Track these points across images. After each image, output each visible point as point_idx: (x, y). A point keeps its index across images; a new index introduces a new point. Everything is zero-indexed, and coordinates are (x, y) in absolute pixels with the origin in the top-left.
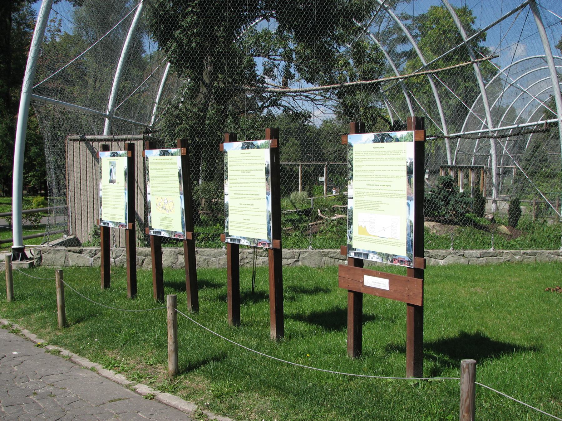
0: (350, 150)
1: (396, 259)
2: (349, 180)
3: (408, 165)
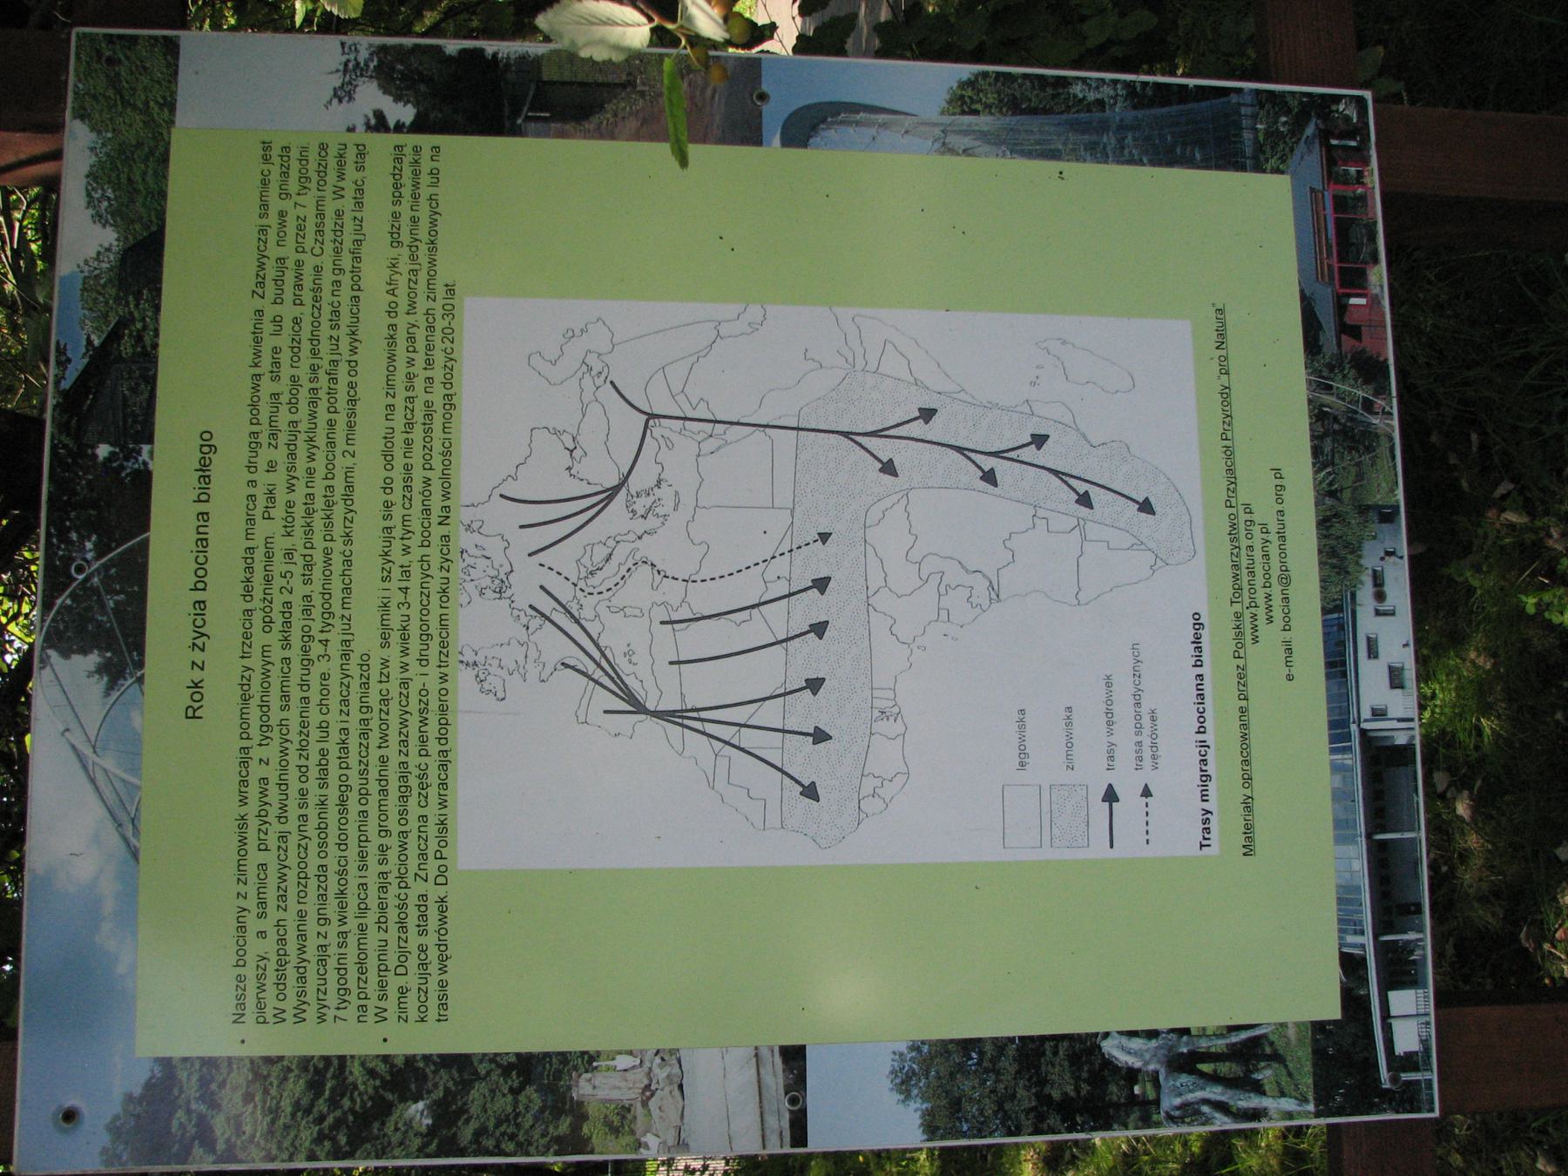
0: (205, 1136)
1: (1341, 308)
2: (577, 1142)
3: (405, 113)
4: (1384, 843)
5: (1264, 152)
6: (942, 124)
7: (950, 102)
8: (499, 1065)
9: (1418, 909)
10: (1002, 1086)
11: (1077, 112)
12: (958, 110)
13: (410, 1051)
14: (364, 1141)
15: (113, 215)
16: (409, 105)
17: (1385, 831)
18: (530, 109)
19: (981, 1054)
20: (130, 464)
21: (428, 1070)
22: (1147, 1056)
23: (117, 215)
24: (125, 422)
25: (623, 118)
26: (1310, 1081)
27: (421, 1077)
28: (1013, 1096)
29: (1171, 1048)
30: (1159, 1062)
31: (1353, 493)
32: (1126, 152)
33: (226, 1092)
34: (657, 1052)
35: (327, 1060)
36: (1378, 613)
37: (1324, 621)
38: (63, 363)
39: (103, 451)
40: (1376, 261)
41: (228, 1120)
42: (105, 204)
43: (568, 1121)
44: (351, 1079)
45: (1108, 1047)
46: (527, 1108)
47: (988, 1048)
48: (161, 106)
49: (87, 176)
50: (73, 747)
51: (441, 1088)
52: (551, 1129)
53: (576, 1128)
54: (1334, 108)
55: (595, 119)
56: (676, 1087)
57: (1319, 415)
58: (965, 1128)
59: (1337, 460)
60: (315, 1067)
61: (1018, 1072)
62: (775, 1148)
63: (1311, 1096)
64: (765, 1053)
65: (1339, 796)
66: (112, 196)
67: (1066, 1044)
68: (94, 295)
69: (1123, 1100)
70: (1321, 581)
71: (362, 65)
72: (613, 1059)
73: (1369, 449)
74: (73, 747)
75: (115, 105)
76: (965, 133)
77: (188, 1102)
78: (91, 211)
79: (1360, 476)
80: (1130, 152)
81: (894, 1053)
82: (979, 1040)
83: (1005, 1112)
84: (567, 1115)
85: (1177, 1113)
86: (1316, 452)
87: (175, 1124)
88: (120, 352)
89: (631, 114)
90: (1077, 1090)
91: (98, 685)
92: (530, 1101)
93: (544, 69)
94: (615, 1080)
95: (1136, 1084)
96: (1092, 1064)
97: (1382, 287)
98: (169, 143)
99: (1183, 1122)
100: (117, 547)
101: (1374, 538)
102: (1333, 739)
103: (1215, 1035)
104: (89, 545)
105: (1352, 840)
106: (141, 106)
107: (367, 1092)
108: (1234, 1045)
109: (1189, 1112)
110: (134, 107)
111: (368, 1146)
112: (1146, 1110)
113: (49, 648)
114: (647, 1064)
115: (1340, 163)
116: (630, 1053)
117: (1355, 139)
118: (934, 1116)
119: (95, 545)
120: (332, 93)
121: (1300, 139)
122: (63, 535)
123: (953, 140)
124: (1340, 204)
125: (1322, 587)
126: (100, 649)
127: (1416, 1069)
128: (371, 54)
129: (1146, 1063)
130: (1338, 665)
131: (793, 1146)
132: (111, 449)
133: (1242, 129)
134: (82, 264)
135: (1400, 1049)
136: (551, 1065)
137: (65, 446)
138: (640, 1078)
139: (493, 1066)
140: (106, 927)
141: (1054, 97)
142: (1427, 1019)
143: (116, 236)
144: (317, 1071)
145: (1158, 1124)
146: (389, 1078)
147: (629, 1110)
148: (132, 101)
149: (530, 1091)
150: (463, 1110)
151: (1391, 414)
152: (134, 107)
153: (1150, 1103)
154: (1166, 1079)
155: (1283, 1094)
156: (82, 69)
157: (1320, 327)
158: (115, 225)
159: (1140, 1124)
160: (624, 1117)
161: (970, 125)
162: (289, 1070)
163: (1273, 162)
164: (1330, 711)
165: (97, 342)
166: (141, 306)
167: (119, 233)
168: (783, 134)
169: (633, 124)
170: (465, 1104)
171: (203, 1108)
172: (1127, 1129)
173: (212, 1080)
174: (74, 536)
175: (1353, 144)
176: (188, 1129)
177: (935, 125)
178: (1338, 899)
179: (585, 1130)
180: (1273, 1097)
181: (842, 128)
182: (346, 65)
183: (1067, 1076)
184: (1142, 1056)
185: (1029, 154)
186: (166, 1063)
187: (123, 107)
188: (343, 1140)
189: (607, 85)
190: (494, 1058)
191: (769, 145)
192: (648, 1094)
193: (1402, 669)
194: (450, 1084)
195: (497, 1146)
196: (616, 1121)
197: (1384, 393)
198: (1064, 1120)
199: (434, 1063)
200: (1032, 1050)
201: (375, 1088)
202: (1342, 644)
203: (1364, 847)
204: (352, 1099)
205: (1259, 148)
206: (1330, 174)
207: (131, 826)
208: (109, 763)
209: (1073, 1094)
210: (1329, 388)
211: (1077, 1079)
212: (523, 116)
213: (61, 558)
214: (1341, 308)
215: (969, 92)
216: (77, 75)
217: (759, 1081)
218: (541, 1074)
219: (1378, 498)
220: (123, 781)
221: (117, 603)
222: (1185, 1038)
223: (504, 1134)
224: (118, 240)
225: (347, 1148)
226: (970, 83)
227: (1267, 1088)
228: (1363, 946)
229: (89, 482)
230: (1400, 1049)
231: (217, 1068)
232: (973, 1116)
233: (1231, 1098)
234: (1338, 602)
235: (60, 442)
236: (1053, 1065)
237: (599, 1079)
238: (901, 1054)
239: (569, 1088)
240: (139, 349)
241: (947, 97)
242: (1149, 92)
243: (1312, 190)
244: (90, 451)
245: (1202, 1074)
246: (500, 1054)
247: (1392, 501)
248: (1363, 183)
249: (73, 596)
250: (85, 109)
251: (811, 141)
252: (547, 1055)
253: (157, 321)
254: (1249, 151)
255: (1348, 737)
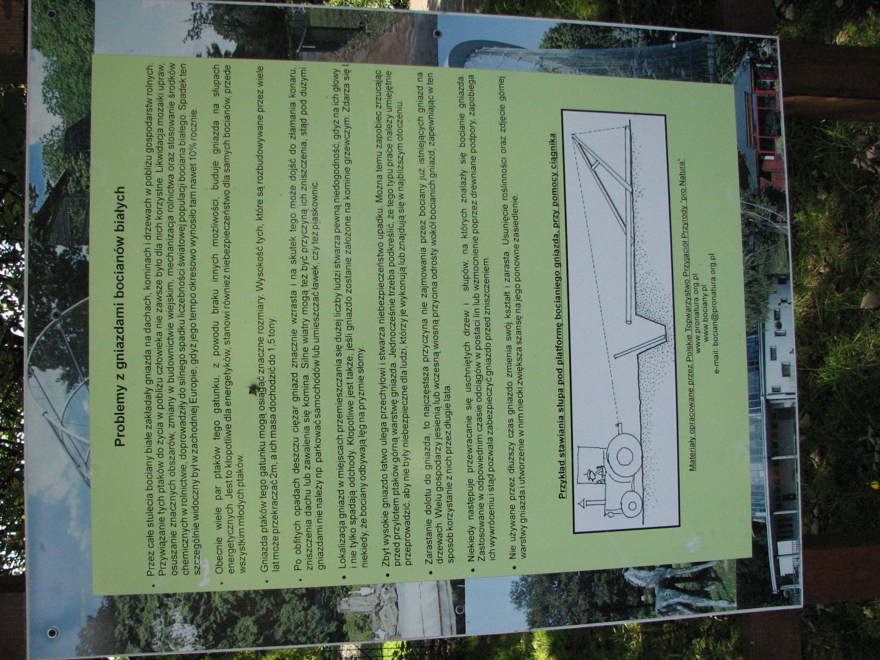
1: (760, 162)
3: (231, 46)
4: (777, 461)
5: (719, 71)
6: (540, 54)
7: (545, 41)
8: (296, 595)
9: (794, 497)
10: (570, 599)
11: (616, 47)
12: (549, 45)
13: (247, 588)
14: (224, 638)
15: (59, 108)
16: (233, 41)
17: (778, 455)
18: (304, 44)
19: (560, 582)
20: (75, 257)
21: (257, 599)
22: (649, 580)
23: (63, 108)
24: (72, 232)
25: (358, 50)
26: (735, 591)
27: (253, 603)
28: (576, 604)
29: (661, 575)
30: (655, 583)
31: (764, 267)
32: (643, 71)
33: (145, 614)
34: (384, 585)
35: (201, 595)
36: (777, 335)
37: (747, 339)
38: (34, 197)
39: (60, 249)
40: (780, 134)
41: (146, 629)
42: (54, 101)
43: (335, 624)
44: (214, 605)
45: (628, 576)
46: (312, 618)
47: (563, 578)
48: (86, 41)
49: (43, 84)
50: (50, 423)
51: (265, 608)
52: (326, 629)
53: (339, 628)
54: (759, 45)
55: (342, 50)
56: (394, 603)
57: (747, 223)
58: (551, 621)
59: (756, 249)
60: (194, 598)
61: (579, 591)
62: (447, 635)
63: (735, 600)
64: (442, 583)
65: (753, 436)
66: (58, 96)
67: (605, 575)
68: (51, 156)
69: (635, 604)
70: (746, 317)
71: (204, 16)
72: (359, 590)
73: (774, 242)
74: (50, 423)
75: (58, 40)
76: (554, 59)
77: (124, 620)
78: (46, 106)
79: (768, 258)
80: (646, 72)
81: (513, 582)
82: (559, 574)
83: (572, 612)
84: (334, 621)
85: (664, 610)
86: (745, 244)
87: (117, 632)
88: (67, 190)
89: (362, 47)
90: (611, 599)
91: (62, 387)
92: (314, 614)
93: (311, 19)
94: (361, 601)
95: (642, 594)
96: (619, 585)
97: (783, 149)
98: (91, 64)
99: (668, 615)
100: (69, 307)
101: (776, 292)
102: (751, 405)
103: (685, 567)
104: (54, 305)
105: (760, 460)
106: (73, 40)
107: (223, 611)
108: (696, 572)
109: (670, 609)
110: (69, 42)
111: (225, 641)
112: (648, 609)
113: (33, 365)
114: (378, 592)
115: (761, 77)
116: (369, 586)
117: (769, 63)
118: (534, 616)
119: (58, 305)
120: (187, 33)
121: (739, 64)
122: (38, 299)
123: (546, 63)
124: (761, 101)
125: (747, 321)
126: (63, 365)
127: (791, 583)
128: (210, 10)
129: (648, 584)
130: (754, 364)
131: (458, 633)
132: (65, 248)
133: (707, 57)
134: (42, 138)
135: (783, 572)
136: (325, 594)
137: (37, 247)
138: (374, 600)
139: (293, 595)
140: (73, 524)
141: (604, 38)
142: (798, 556)
143: (61, 120)
144: (195, 601)
145: (655, 616)
146: (235, 604)
147: (368, 617)
148: (68, 38)
149: (314, 608)
150: (277, 620)
151: (786, 222)
152: (69, 42)
153: (649, 605)
154: (659, 591)
155: (720, 599)
156: (36, 18)
157: (749, 173)
158: (61, 114)
159: (644, 616)
160: (365, 621)
161: (556, 55)
162: (180, 601)
163: (724, 77)
164: (750, 390)
165: (53, 185)
166: (79, 163)
167: (63, 118)
168: (450, 60)
169: (364, 53)
170: (278, 616)
171: (132, 623)
172: (637, 618)
173: (136, 608)
174: (45, 300)
175: (769, 66)
176: (125, 634)
177: (535, 54)
178: (752, 493)
179: (345, 628)
180: (716, 600)
181: (484, 57)
182: (195, 17)
183: (606, 592)
184: (646, 580)
185: (590, 72)
186: (110, 599)
187: (62, 41)
188: (211, 638)
189: (348, 29)
190: (293, 591)
191: (443, 66)
192: (379, 608)
193: (789, 366)
194: (270, 606)
195: (296, 639)
196: (361, 623)
197: (782, 211)
198: (603, 616)
199: (261, 595)
200: (587, 579)
201: (228, 609)
202: (758, 352)
203: (766, 463)
204: (215, 615)
205: (717, 69)
206: (755, 82)
207: (85, 467)
208: (71, 431)
209: (608, 602)
210: (753, 207)
211: (611, 593)
212: (300, 48)
213: (38, 313)
214: (760, 162)
215: (556, 35)
216: (33, 21)
217: (439, 599)
218: (320, 599)
219: (778, 270)
220: (80, 441)
221: (71, 339)
222: (669, 570)
223: (299, 633)
224: (63, 123)
225: (213, 643)
226: (556, 30)
227: (712, 595)
228: (765, 518)
229: (52, 268)
230: (783, 572)
231: (139, 601)
232: (555, 615)
233: (693, 601)
234: (755, 329)
235: (34, 245)
236: (598, 587)
237: (352, 601)
238: (517, 583)
239: (335, 606)
240: (78, 189)
241: (544, 38)
242: (656, 35)
243: (746, 93)
244: (52, 250)
245: (678, 589)
246: (297, 589)
247: (785, 272)
248: (773, 89)
249: (45, 335)
250: (39, 42)
251: (466, 63)
252: (323, 588)
253: (88, 171)
254: (711, 71)
255: (759, 404)
